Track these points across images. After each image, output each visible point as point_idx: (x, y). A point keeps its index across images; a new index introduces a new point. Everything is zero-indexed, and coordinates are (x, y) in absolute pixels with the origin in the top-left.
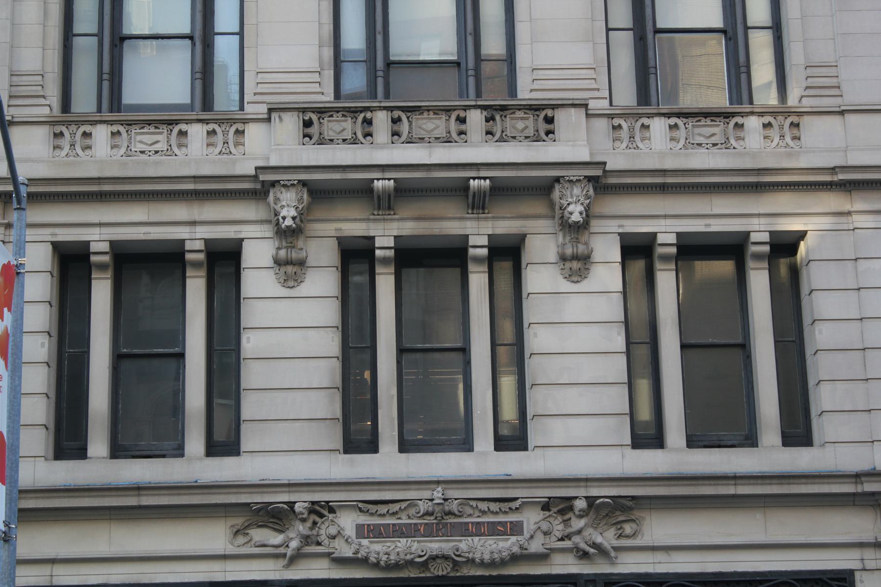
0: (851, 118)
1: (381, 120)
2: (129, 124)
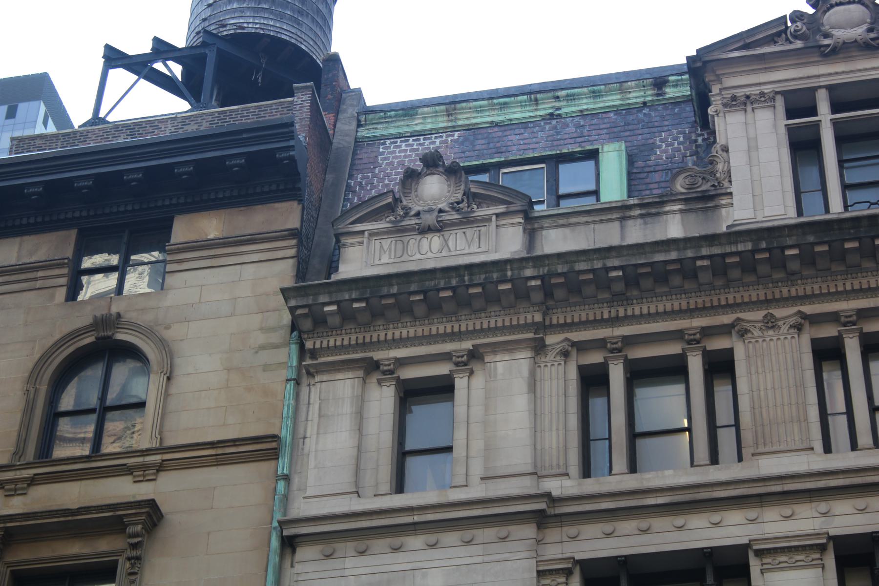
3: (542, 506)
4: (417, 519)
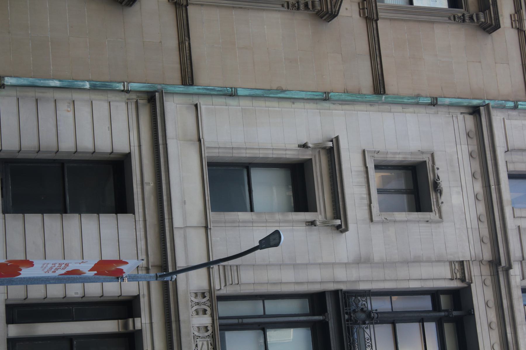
2: (213, 336)
3: (503, 263)
4: (493, 187)
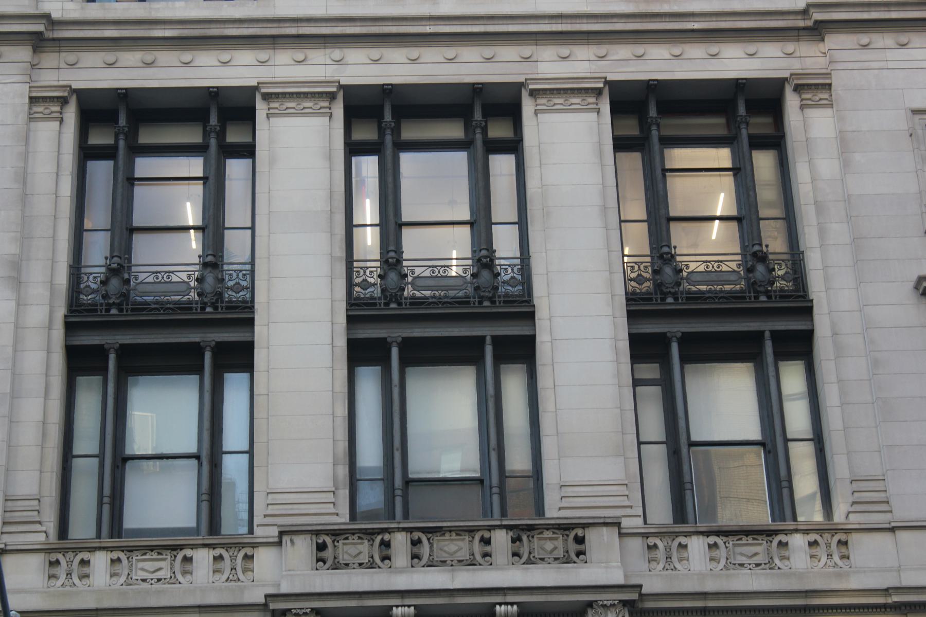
0: (903, 535)
1: (400, 542)
2: (130, 550)
3: (40, 28)
